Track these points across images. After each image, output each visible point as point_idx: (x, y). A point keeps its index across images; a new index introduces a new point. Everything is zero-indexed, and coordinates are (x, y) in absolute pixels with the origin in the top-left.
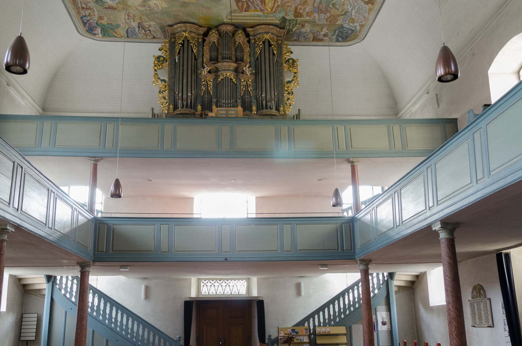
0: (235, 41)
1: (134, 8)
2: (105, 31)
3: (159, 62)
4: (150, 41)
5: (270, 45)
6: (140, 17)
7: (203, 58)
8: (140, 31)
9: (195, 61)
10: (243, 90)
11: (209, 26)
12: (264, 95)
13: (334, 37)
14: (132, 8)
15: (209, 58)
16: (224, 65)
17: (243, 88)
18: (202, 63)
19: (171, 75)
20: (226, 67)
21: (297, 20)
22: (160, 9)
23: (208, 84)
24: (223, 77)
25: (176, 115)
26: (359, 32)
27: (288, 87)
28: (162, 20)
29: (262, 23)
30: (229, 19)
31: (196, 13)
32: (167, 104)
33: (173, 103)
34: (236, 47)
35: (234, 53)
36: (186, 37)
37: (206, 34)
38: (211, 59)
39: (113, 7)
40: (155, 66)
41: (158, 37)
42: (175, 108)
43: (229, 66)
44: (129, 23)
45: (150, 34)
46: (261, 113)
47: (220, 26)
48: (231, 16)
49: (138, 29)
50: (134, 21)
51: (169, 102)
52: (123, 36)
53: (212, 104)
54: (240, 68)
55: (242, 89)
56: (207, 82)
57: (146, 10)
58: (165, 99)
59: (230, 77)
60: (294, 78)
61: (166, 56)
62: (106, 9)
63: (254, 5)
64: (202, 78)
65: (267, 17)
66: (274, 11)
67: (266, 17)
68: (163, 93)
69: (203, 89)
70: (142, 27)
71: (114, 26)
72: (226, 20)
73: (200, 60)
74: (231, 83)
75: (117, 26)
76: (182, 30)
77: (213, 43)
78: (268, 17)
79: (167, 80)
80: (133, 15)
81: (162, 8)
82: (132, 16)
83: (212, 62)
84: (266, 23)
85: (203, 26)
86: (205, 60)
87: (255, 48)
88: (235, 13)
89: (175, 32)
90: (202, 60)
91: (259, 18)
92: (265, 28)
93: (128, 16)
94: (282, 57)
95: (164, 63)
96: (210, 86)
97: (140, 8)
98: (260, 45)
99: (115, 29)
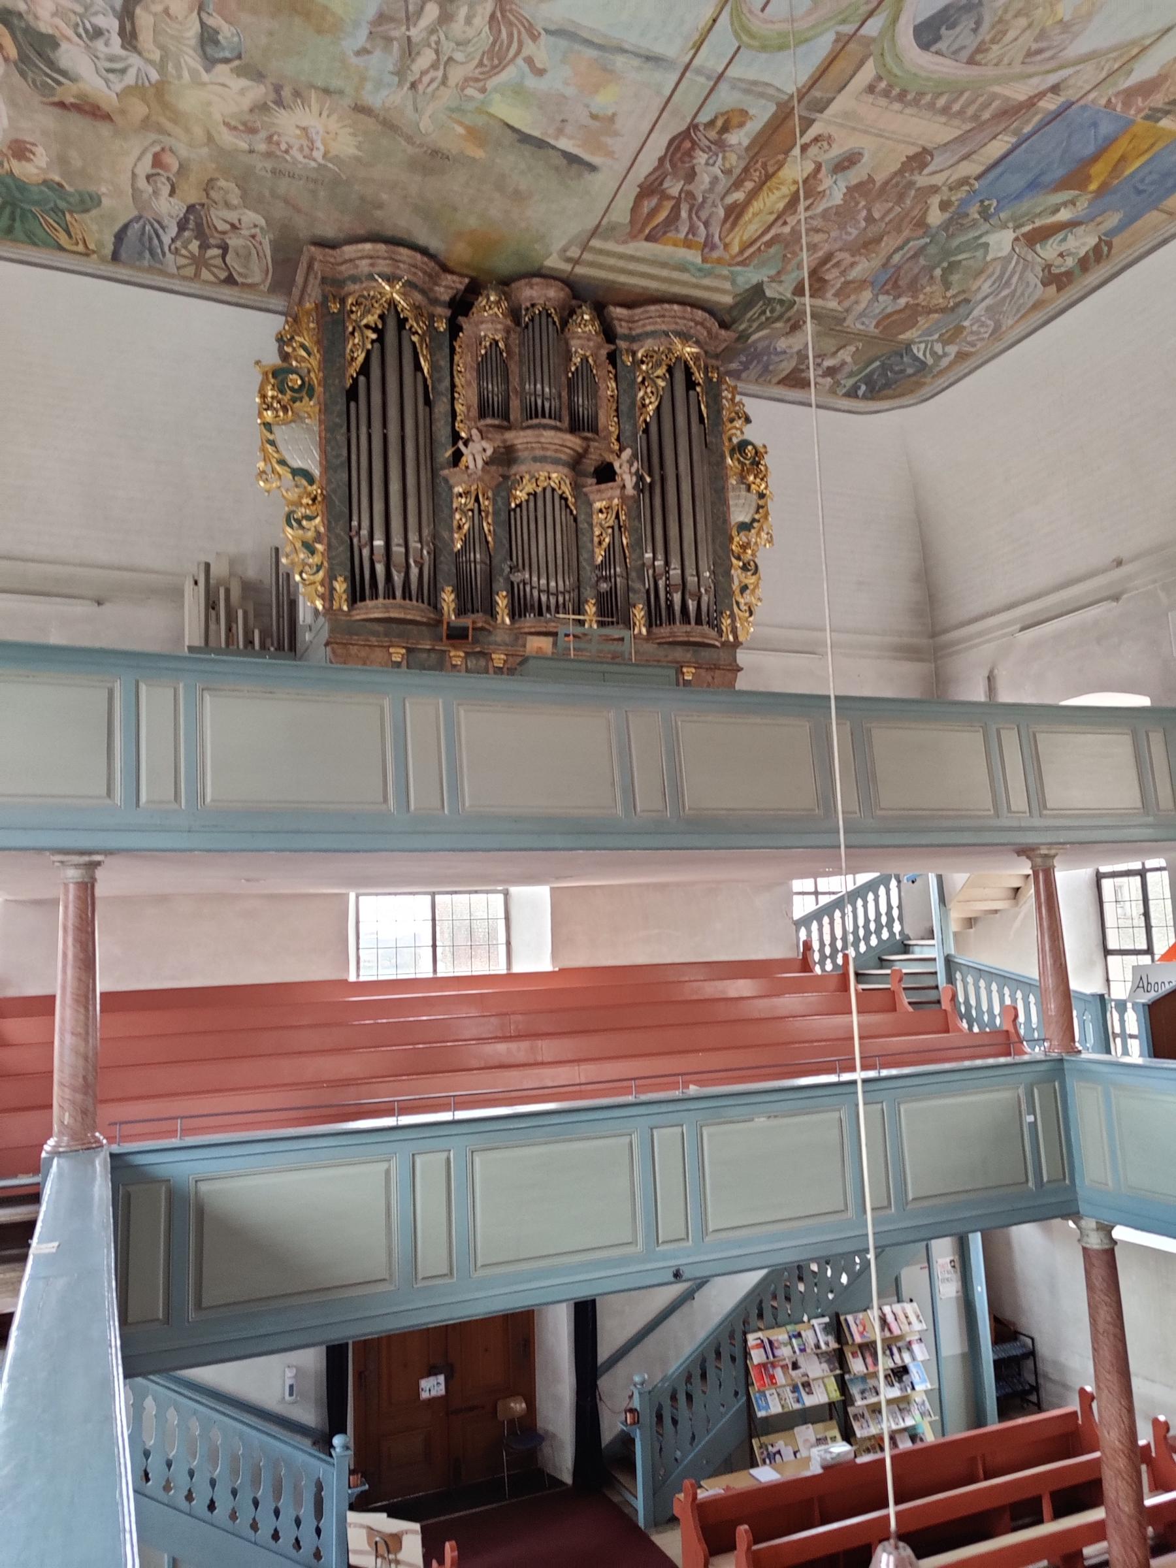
0: (569, 351)
1: (198, 131)
2: (19, 211)
3: (282, 392)
4: (209, 291)
5: (691, 384)
6: (211, 180)
7: (453, 398)
8: (178, 244)
9: (424, 410)
10: (600, 543)
11: (474, 274)
12: (675, 573)
13: (850, 382)
14: (187, 130)
15: (474, 401)
16: (543, 440)
17: (601, 534)
18: (450, 420)
19: (334, 453)
20: (547, 449)
21: (795, 302)
22: (315, 160)
23: (483, 508)
24: (537, 486)
25: (362, 623)
26: (933, 377)
27: (745, 547)
28: (298, 210)
29: (675, 295)
30: (568, 260)
31: (455, 209)
32: (321, 574)
33: (348, 574)
34: (573, 374)
35: (564, 394)
36: (392, 304)
37: (461, 306)
38: (484, 410)
39: (99, 108)
40: (266, 410)
41: (249, 281)
42: (356, 595)
43: (562, 446)
44: (145, 196)
45: (219, 261)
46: (669, 637)
47: (523, 282)
48: (585, 247)
49: (173, 230)
50: (172, 193)
51: (330, 564)
52: (94, 252)
53: (495, 587)
54: (590, 456)
55: (596, 540)
56: (477, 500)
57: (251, 152)
58: (312, 552)
59: (560, 488)
60: (757, 512)
61: (309, 372)
62: (57, 111)
63: (698, 217)
64: (452, 482)
65: (705, 276)
66: (746, 259)
67: (701, 274)
68: (301, 527)
69: (460, 527)
70: (199, 227)
71: (71, 200)
72: (554, 262)
73: (441, 407)
74: (563, 513)
75: (82, 201)
76: (377, 269)
77: (491, 345)
78: (709, 274)
79: (316, 472)
80: (181, 166)
81: (330, 155)
82: (175, 167)
83: (489, 421)
84: (687, 296)
85: (457, 270)
86: (459, 408)
87: (633, 386)
88: (605, 239)
89: (340, 273)
90: (448, 407)
91: (675, 275)
92: (678, 314)
93: (157, 162)
94: (721, 433)
95: (301, 400)
96: (487, 517)
97: (227, 139)
98: (658, 377)
99: (71, 212)
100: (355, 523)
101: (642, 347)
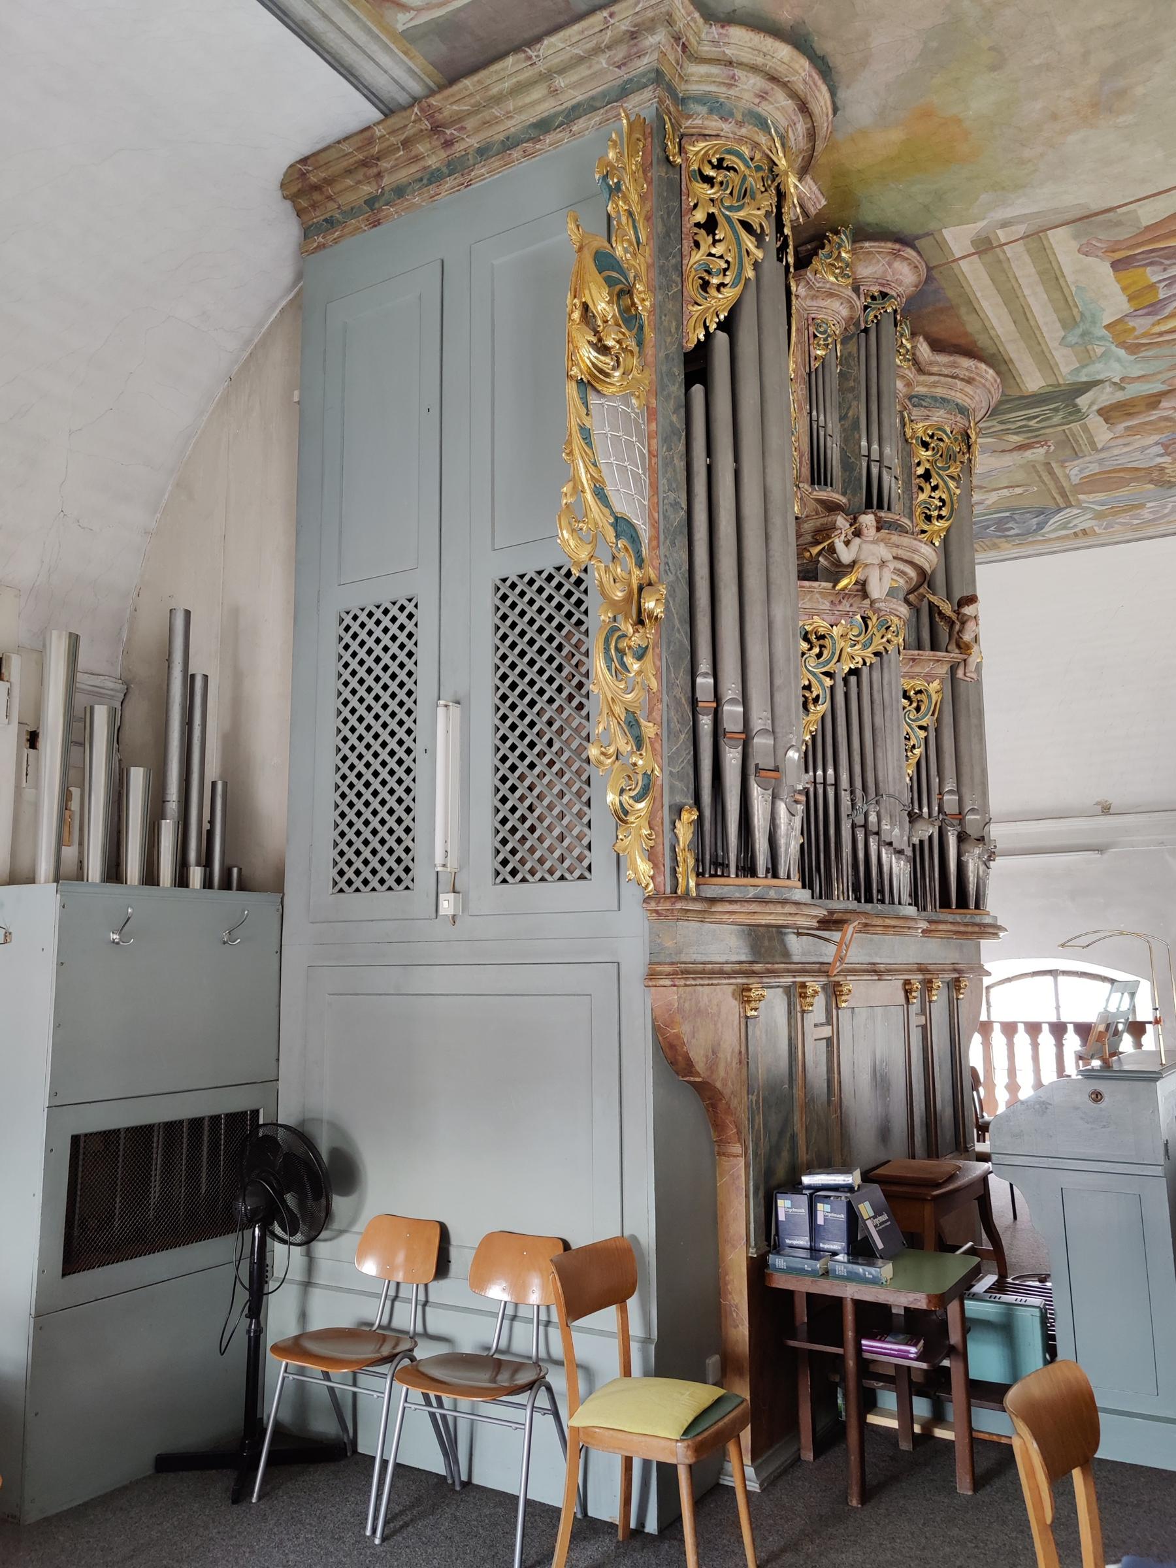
100: (704, 682)
101: (927, 417)
